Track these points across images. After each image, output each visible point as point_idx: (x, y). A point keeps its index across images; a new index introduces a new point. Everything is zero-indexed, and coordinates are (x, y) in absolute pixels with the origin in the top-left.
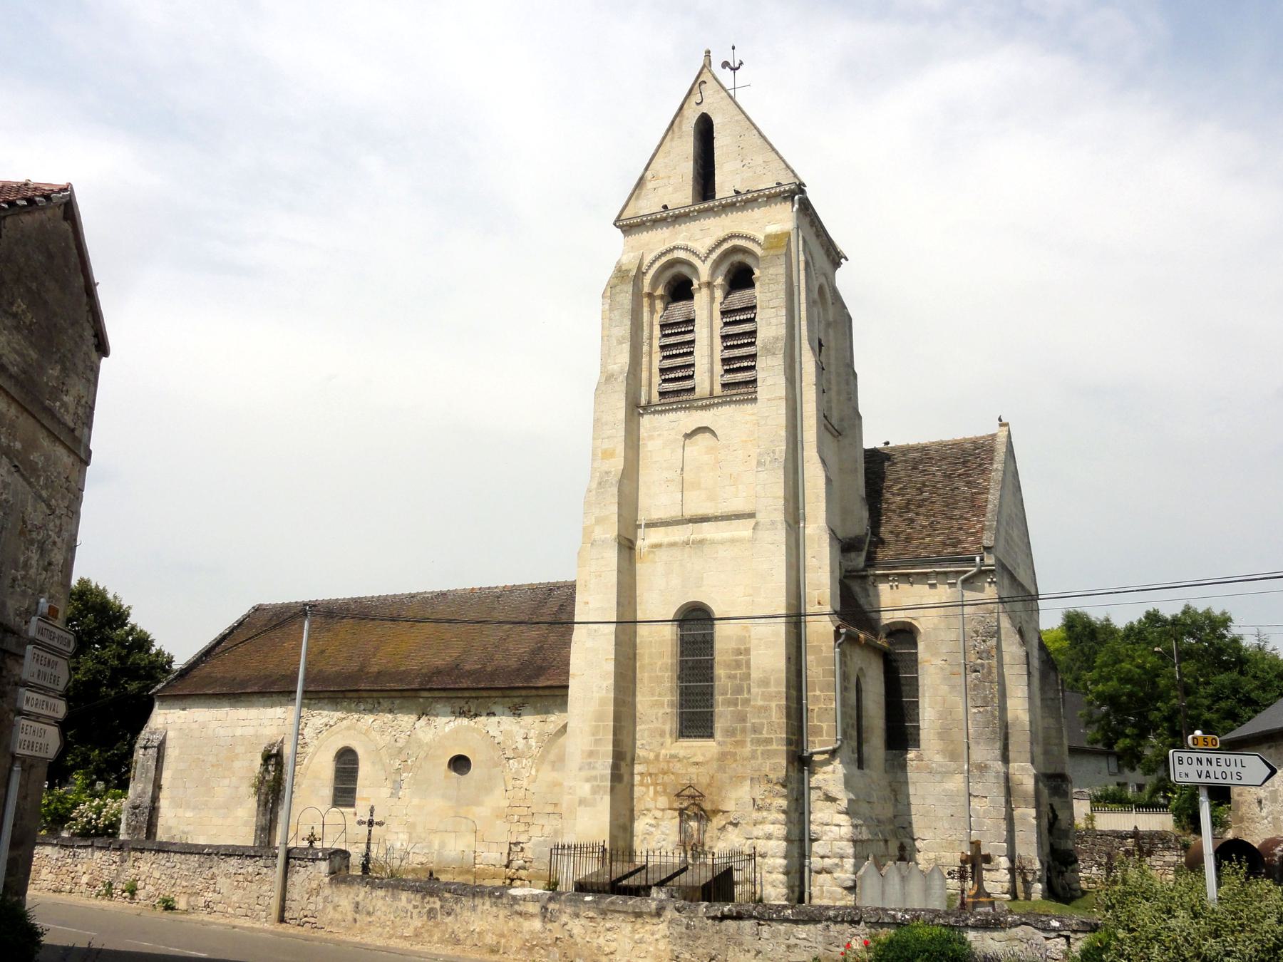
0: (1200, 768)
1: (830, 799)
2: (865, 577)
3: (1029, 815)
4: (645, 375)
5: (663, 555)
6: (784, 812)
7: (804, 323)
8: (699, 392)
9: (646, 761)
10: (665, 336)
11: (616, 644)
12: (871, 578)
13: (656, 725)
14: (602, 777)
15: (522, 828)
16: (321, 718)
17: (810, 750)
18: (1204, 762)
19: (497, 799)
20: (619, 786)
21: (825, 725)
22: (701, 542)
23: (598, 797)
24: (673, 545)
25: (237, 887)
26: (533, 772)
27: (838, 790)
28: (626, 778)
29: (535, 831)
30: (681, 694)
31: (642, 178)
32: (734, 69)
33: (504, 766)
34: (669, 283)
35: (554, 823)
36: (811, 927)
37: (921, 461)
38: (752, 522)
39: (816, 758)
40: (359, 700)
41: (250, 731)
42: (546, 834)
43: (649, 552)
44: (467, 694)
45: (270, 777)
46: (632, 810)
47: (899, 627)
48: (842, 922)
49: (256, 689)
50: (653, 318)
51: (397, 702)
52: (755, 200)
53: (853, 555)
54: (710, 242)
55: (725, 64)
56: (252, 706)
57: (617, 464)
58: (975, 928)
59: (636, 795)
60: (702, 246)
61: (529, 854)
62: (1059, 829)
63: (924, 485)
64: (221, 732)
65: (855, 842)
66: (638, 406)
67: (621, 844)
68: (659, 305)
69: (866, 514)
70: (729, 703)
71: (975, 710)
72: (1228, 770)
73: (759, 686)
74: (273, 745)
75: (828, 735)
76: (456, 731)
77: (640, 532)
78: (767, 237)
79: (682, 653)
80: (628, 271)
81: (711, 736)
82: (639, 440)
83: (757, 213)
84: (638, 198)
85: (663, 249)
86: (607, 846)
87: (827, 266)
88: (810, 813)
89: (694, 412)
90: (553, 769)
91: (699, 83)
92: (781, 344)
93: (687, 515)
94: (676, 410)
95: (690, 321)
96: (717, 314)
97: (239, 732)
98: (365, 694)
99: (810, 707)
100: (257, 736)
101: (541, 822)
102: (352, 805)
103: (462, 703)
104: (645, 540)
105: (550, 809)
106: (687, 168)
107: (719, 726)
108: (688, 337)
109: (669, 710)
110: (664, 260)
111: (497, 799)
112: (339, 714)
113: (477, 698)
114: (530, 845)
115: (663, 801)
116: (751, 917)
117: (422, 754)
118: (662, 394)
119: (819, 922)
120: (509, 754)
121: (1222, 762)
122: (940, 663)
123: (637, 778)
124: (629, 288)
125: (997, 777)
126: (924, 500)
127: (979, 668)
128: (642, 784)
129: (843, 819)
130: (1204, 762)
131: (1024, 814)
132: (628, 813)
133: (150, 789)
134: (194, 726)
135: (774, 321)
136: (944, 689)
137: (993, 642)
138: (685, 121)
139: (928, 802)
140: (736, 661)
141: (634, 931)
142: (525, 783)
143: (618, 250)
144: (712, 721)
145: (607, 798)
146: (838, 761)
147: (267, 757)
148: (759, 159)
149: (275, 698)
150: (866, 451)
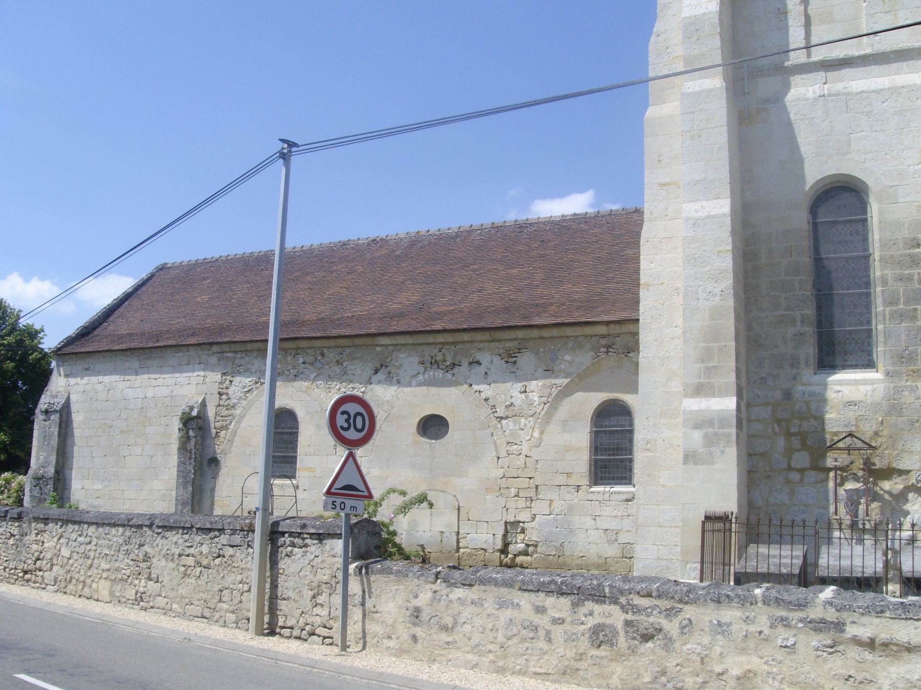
15: (522, 503)
19: (486, 469)
25: (185, 575)
26: (536, 434)
29: (540, 507)
33: (495, 427)
35: (568, 496)
42: (556, 511)
44: (441, 338)
61: (533, 536)
70: (901, 316)
81: (870, 364)
90: (564, 429)
98: (304, 344)
102: (292, 476)
103: (436, 351)
105: (561, 480)
107: (880, 350)
111: (486, 469)
113: (454, 343)
120: (501, 412)
133: (53, 459)
140: (911, 256)
142: (525, 449)
144: (870, 344)
149: (192, 352)
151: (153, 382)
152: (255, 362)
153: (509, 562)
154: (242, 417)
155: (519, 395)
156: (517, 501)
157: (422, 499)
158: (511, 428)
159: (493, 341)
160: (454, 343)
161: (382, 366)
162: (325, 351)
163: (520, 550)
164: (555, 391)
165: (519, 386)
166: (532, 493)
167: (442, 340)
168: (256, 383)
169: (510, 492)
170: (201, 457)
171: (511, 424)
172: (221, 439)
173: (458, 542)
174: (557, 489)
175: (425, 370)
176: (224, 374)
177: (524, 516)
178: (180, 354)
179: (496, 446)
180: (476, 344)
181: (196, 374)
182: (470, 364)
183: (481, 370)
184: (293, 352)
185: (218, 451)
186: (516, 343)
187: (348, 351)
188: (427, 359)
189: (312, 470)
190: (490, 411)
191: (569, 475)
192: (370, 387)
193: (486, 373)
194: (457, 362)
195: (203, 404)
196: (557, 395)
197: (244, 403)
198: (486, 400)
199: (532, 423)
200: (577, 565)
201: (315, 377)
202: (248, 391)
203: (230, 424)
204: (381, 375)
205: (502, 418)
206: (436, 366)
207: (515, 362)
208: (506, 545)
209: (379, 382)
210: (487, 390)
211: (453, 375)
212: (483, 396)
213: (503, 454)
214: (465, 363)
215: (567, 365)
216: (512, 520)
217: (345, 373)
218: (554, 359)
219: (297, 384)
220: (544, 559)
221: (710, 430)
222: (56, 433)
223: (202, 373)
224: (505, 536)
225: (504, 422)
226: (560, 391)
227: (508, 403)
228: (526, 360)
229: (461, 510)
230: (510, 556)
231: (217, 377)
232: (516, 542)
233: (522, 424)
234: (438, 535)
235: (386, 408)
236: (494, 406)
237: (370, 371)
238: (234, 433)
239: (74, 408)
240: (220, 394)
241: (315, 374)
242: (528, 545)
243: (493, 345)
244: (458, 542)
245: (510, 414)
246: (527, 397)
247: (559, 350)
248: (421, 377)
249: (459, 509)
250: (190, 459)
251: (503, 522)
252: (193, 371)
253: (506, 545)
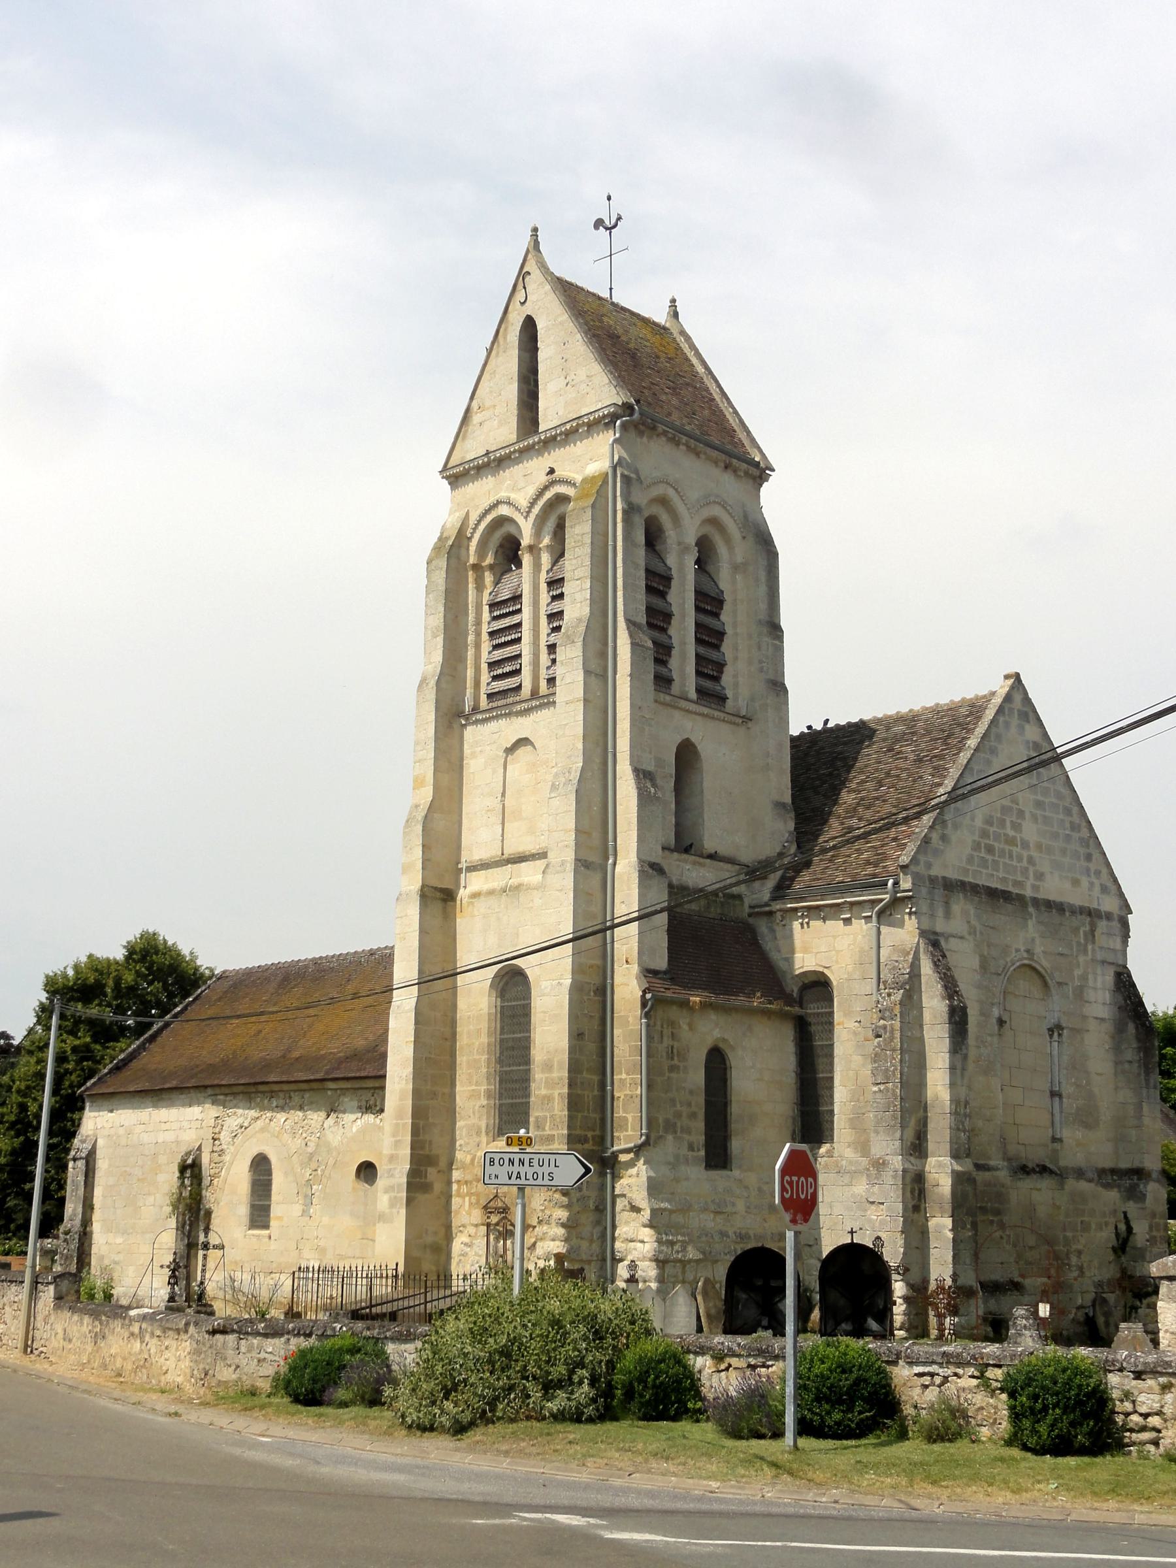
0: (511, 1169)
1: (635, 1209)
2: (771, 914)
3: (944, 1226)
4: (470, 673)
5: (481, 906)
6: (563, 1225)
7: (620, 594)
8: (526, 691)
9: (463, 1167)
10: (495, 618)
11: (417, 1023)
12: (779, 914)
13: (473, 1121)
14: (399, 1185)
16: (238, 1116)
17: (615, 1148)
18: (516, 1162)
20: (421, 1197)
21: (630, 1117)
22: (518, 888)
23: (395, 1210)
24: (491, 893)
27: (640, 1197)
28: (438, 1187)
30: (501, 1082)
31: (468, 410)
32: (610, 229)
34: (501, 546)
36: (276, 1341)
37: (897, 739)
38: (540, 864)
39: (623, 1158)
40: (272, 1094)
41: (170, 1137)
43: (470, 903)
45: (186, 1194)
46: (448, 1227)
47: (814, 978)
48: (298, 1335)
49: (174, 1083)
50: (478, 598)
51: (307, 1095)
52: (574, 431)
53: (757, 884)
54: (531, 491)
55: (599, 223)
56: (171, 1105)
57: (426, 794)
58: (393, 1339)
59: (454, 1207)
60: (523, 500)
62: (1135, 1248)
63: (888, 774)
64: (145, 1138)
65: (656, 1260)
66: (460, 714)
67: (428, 1266)
68: (488, 578)
69: (787, 826)
71: (876, 1089)
72: (540, 1171)
73: (543, 1072)
74: (188, 1153)
75: (633, 1129)
76: (363, 1131)
77: (463, 876)
78: (584, 480)
79: (502, 1028)
80: (447, 538)
82: (462, 759)
83: (580, 448)
84: (464, 439)
85: (486, 505)
86: (401, 1269)
87: (729, 486)
88: (614, 1227)
89: (514, 719)
91: (523, 275)
92: (582, 629)
93: (509, 851)
94: (497, 717)
95: (517, 598)
96: (543, 587)
97: (161, 1138)
98: (276, 1087)
99: (616, 1094)
100: (177, 1142)
104: (473, 884)
106: (512, 391)
108: (515, 619)
109: (485, 1102)
110: (489, 518)
112: (253, 1113)
115: (477, 1215)
116: (233, 1331)
117: (331, 1162)
118: (490, 696)
119: (282, 1335)
121: (535, 1163)
122: (852, 1025)
123: (455, 1187)
124: (443, 563)
125: (895, 1177)
126: (877, 798)
127: (881, 1032)
128: (459, 1195)
129: (647, 1234)
130: (516, 1162)
131: (937, 1225)
132: (443, 1231)
133: (80, 1210)
134: (121, 1131)
135: (578, 596)
136: (857, 1059)
137: (898, 995)
138: (510, 328)
139: (836, 1211)
141: (177, 1349)
143: (438, 509)
145: (403, 1211)
146: (642, 1161)
147: (183, 1169)
148: (582, 373)
149: (193, 1094)
150: (793, 739)
189: (280, 1218)
221: (393, 1194)
235: (334, 1154)
239: (100, 1154)
240: (214, 1139)
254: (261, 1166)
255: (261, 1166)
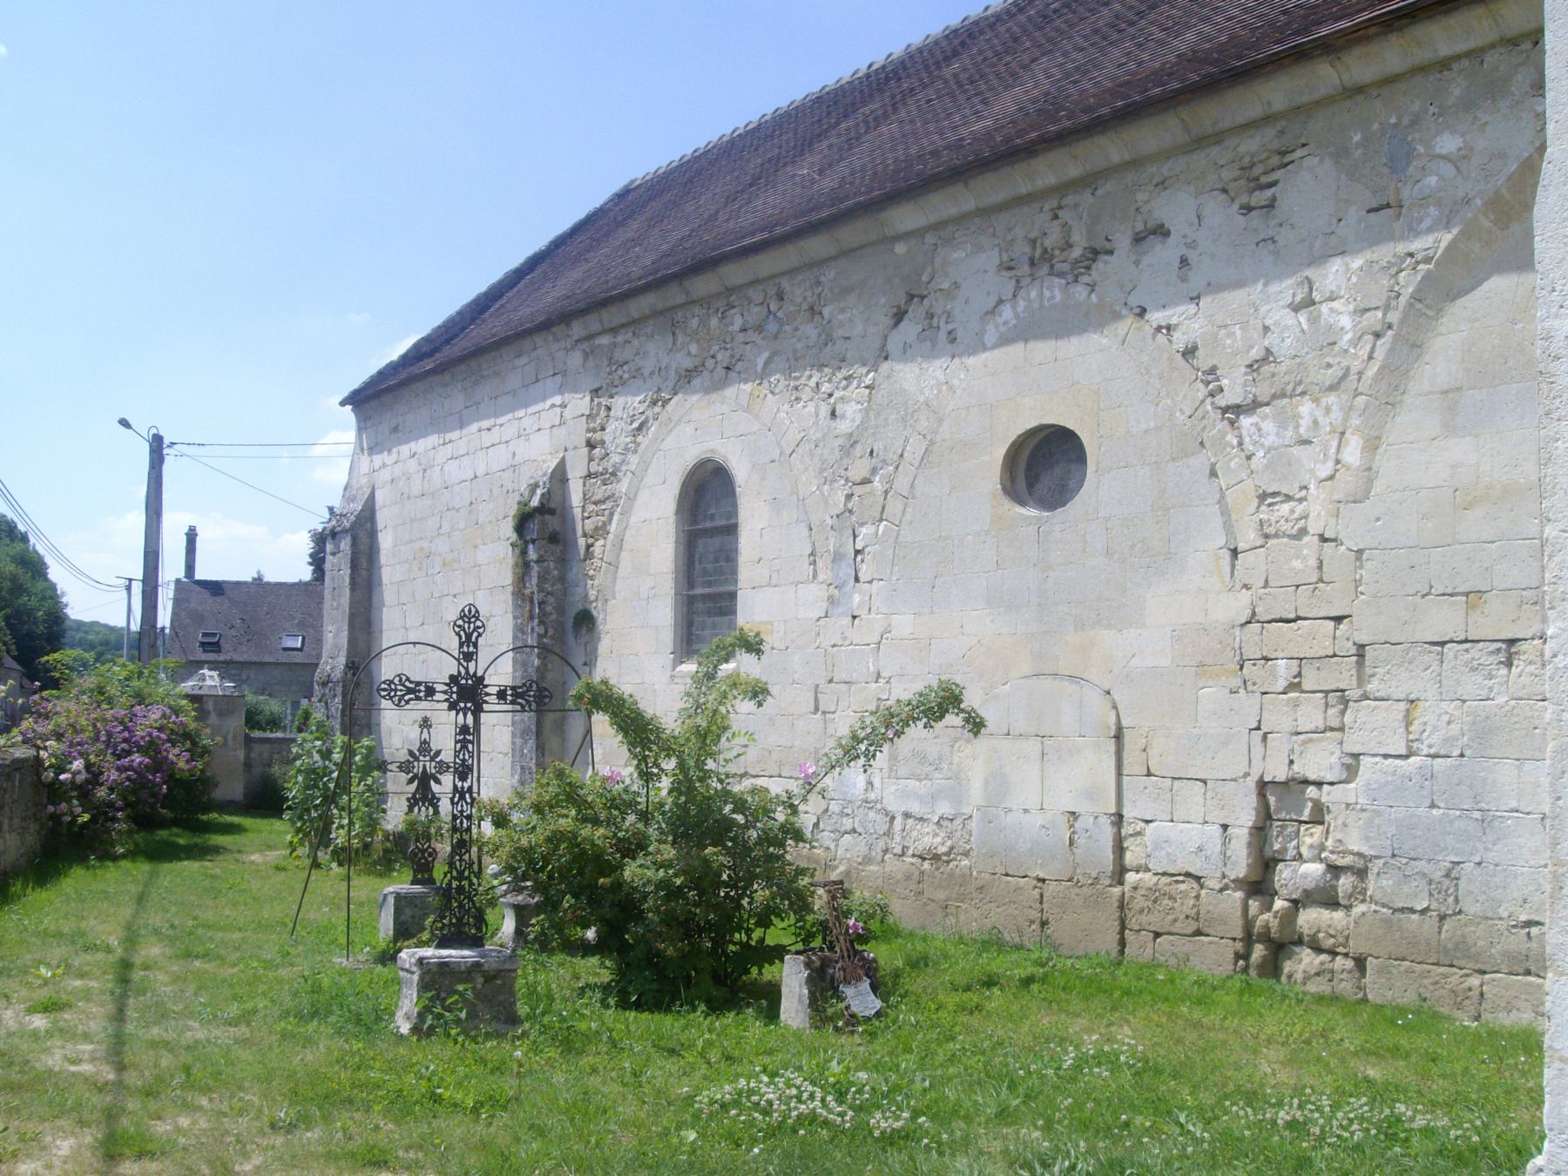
15: (1311, 714)
26: (1352, 453)
29: (1373, 727)
35: (1472, 685)
42: (1432, 740)
90: (1451, 428)
101: (1402, 685)
105: (1446, 620)
111: (1196, 597)
113: (1088, 182)
114: (1350, 792)
117: (915, 448)
120: (1234, 389)
147: (523, 521)
151: (487, 438)
152: (651, 347)
153: (1274, 924)
154: (632, 499)
155: (1289, 319)
156: (1296, 705)
157: (942, 703)
158: (1269, 441)
159: (1199, 143)
160: (1088, 182)
161: (911, 297)
162: (785, 284)
163: (1310, 885)
164: (1408, 283)
165: (1286, 289)
166: (1343, 675)
167: (1051, 179)
168: (654, 403)
169: (1274, 675)
170: (561, 610)
171: (1269, 426)
172: (596, 562)
173: (1119, 849)
174: (1431, 657)
175: (1018, 288)
176: (596, 392)
177: (1319, 762)
178: (523, 360)
179: (1225, 512)
180: (1152, 169)
181: (549, 402)
182: (1138, 239)
183: (1164, 254)
184: (721, 304)
185: (592, 594)
186: (1270, 132)
187: (828, 275)
188: (1022, 250)
190: (1202, 391)
191: (1473, 597)
192: (885, 367)
193: (1184, 262)
194: (1098, 245)
195: (560, 476)
196: (1417, 298)
197: (634, 460)
198: (1189, 352)
199: (1336, 415)
200: (1509, 956)
201: (767, 363)
202: (639, 429)
203: (610, 520)
204: (909, 329)
205: (1238, 409)
206: (1045, 269)
207: (1271, 205)
208: (1265, 866)
209: (906, 353)
210: (1191, 323)
211: (1092, 287)
212: (1180, 340)
213: (1248, 537)
214: (1122, 242)
215: (1448, 170)
216: (1281, 777)
217: (829, 340)
218: (1400, 161)
219: (730, 392)
220: (1387, 922)
222: (347, 580)
223: (557, 400)
224: (1260, 832)
225: (1246, 422)
226: (1428, 276)
227: (1256, 353)
228: (1309, 188)
229: (1128, 736)
230: (1279, 904)
231: (580, 403)
232: (1299, 857)
233: (1305, 423)
234: (1063, 821)
235: (923, 424)
236: (1212, 370)
237: (883, 319)
238: (621, 541)
239: (382, 518)
240: (591, 445)
241: (765, 355)
242: (1335, 870)
243: (1200, 160)
244: (1119, 849)
245: (1263, 392)
246: (1314, 320)
247: (1413, 123)
248: (1007, 312)
249: (1118, 737)
250: (531, 618)
251: (1251, 783)
252: (544, 399)
253: (1265, 866)
254: (707, 497)
255: (707, 497)
